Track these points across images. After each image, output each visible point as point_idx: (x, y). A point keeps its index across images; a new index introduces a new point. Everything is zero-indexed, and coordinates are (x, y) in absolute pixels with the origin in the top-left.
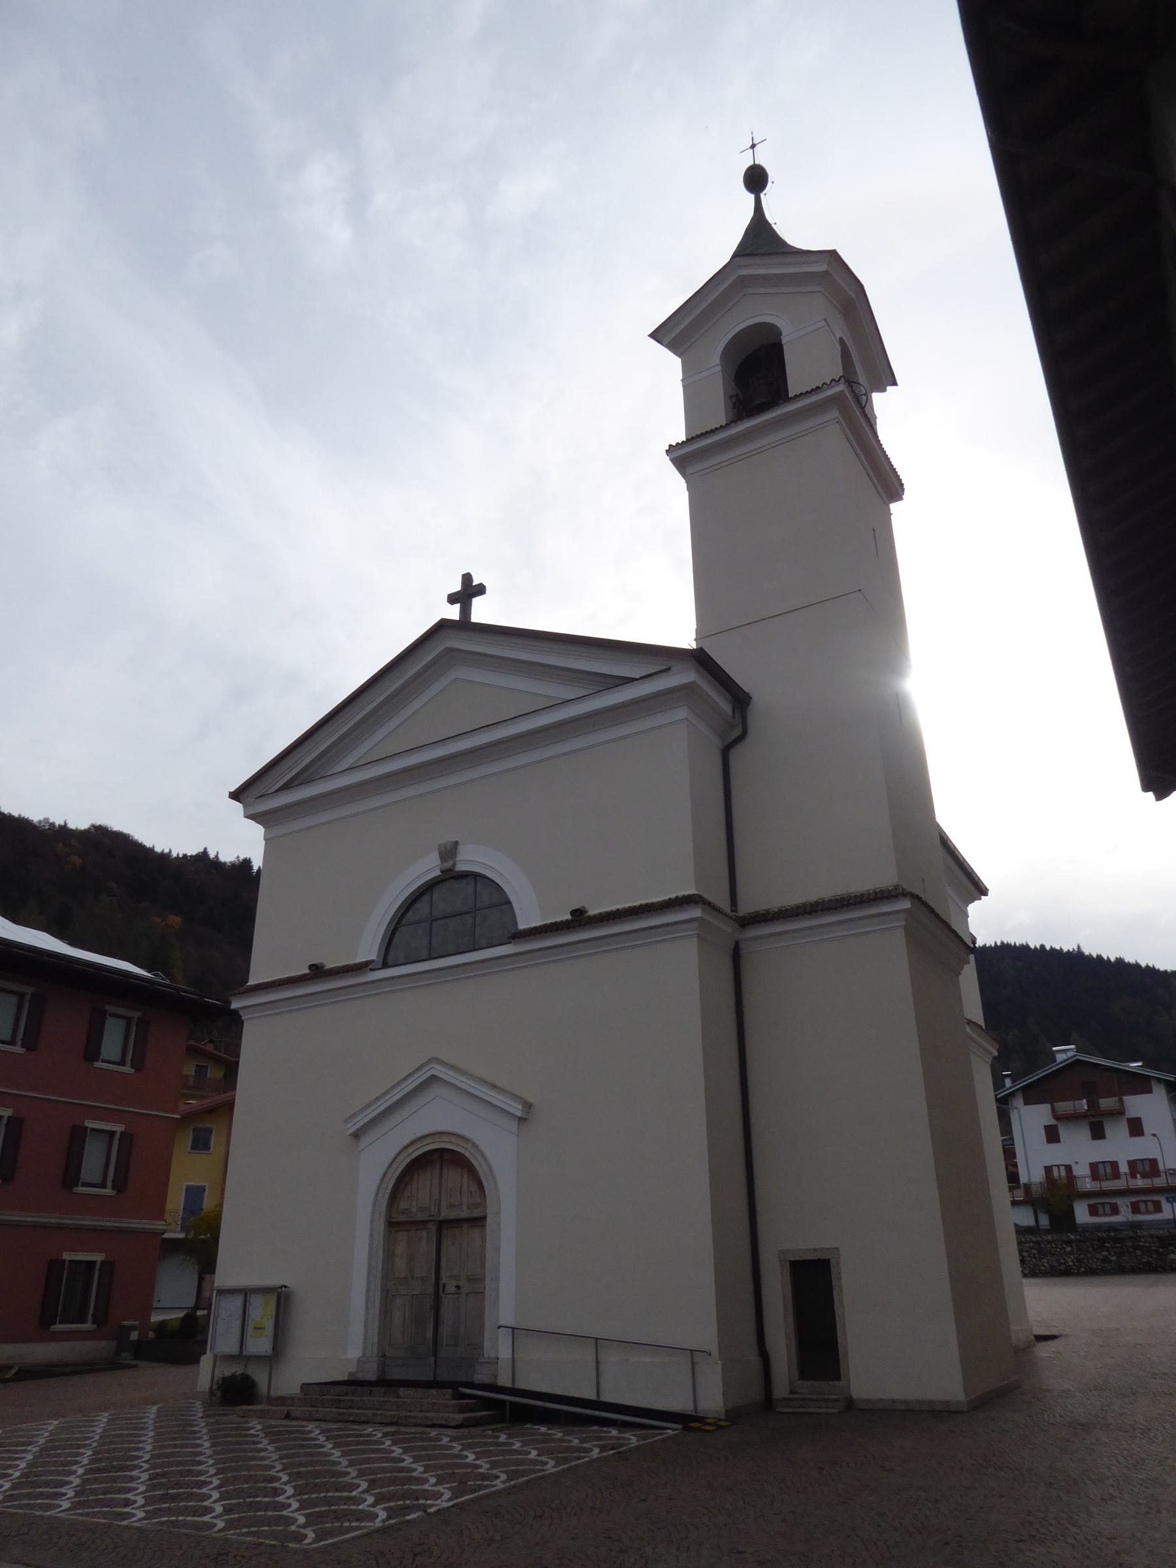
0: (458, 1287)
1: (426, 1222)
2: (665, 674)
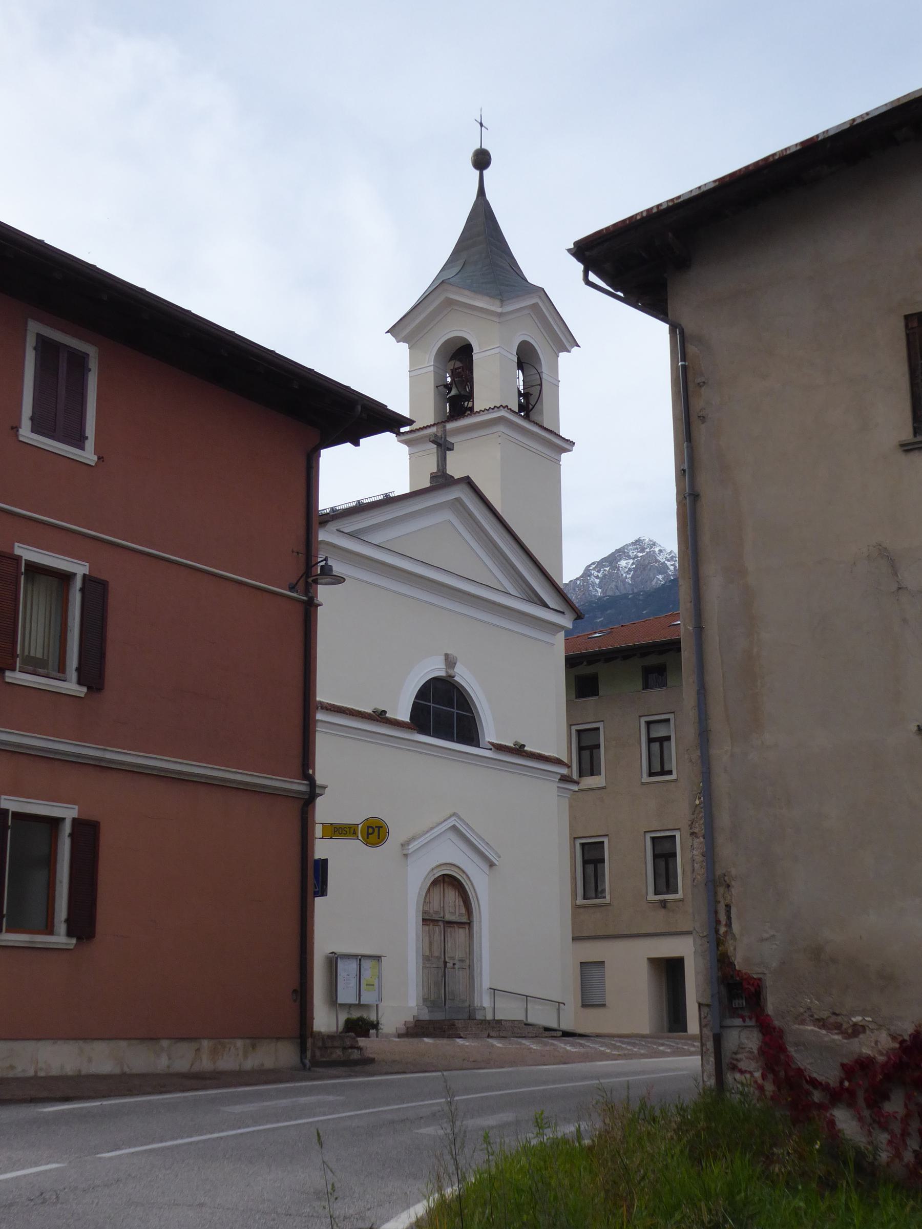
0: (454, 964)
1: (437, 921)
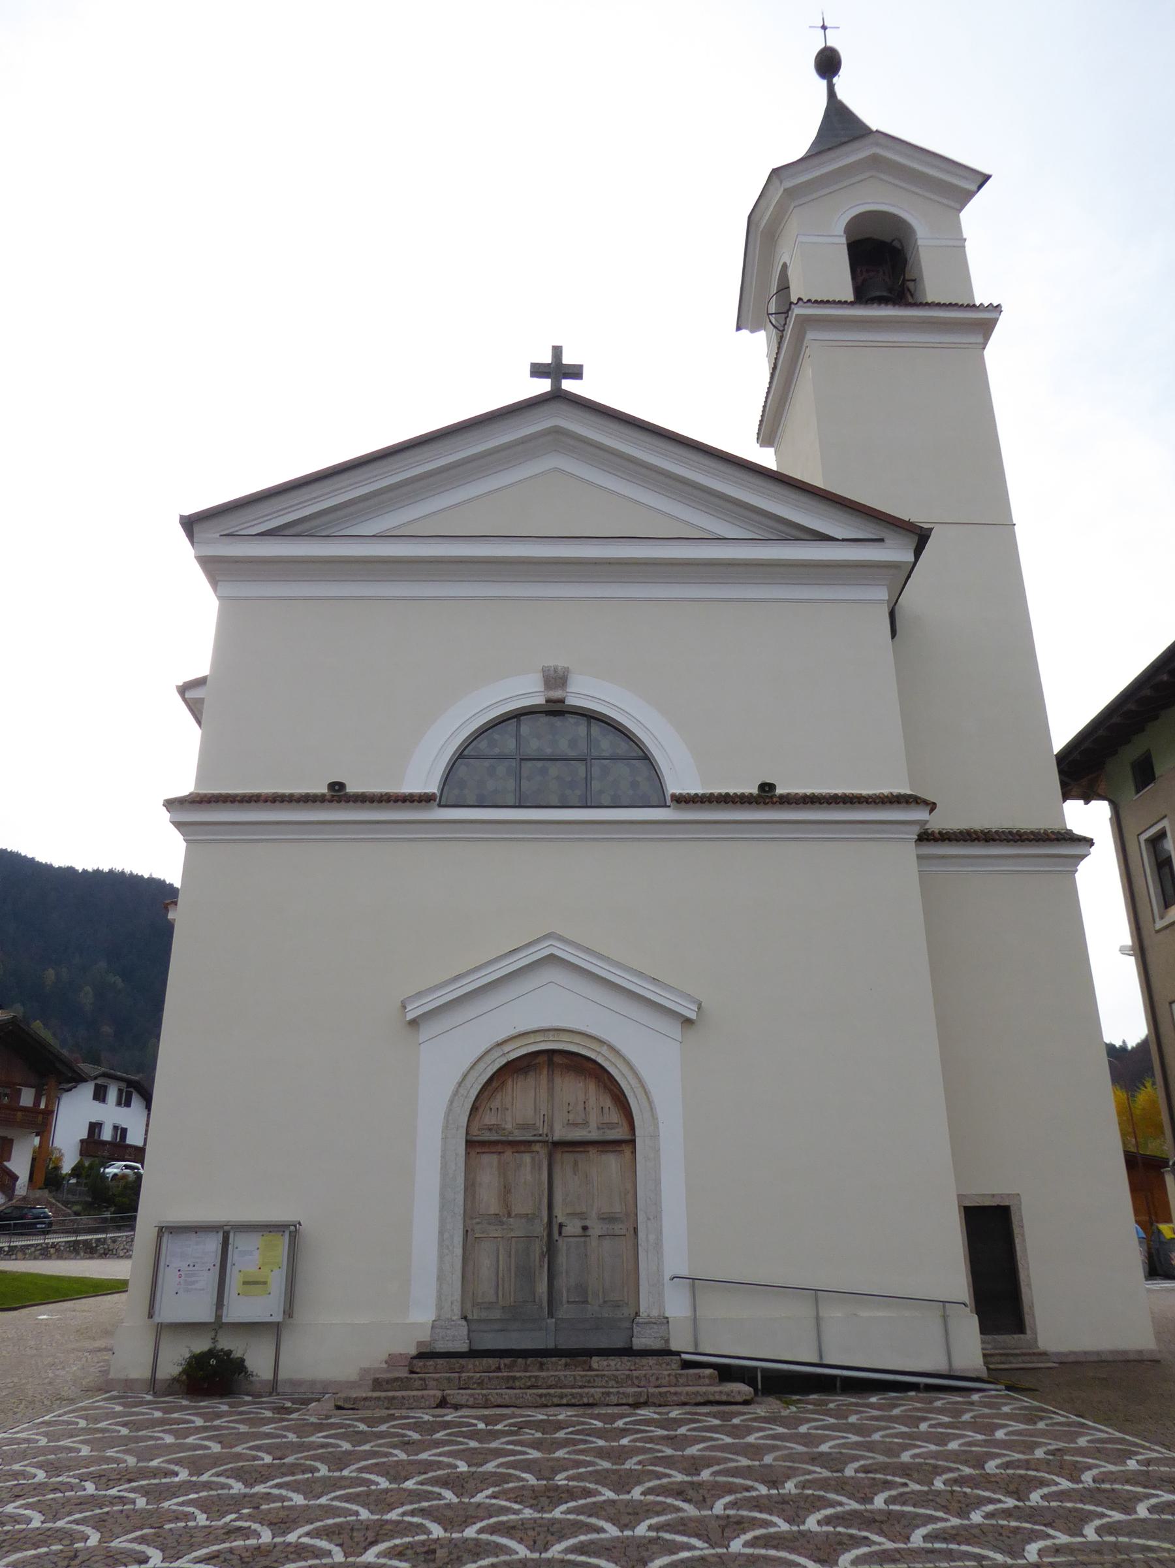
0: (585, 1228)
1: (527, 1145)
2: (877, 544)
